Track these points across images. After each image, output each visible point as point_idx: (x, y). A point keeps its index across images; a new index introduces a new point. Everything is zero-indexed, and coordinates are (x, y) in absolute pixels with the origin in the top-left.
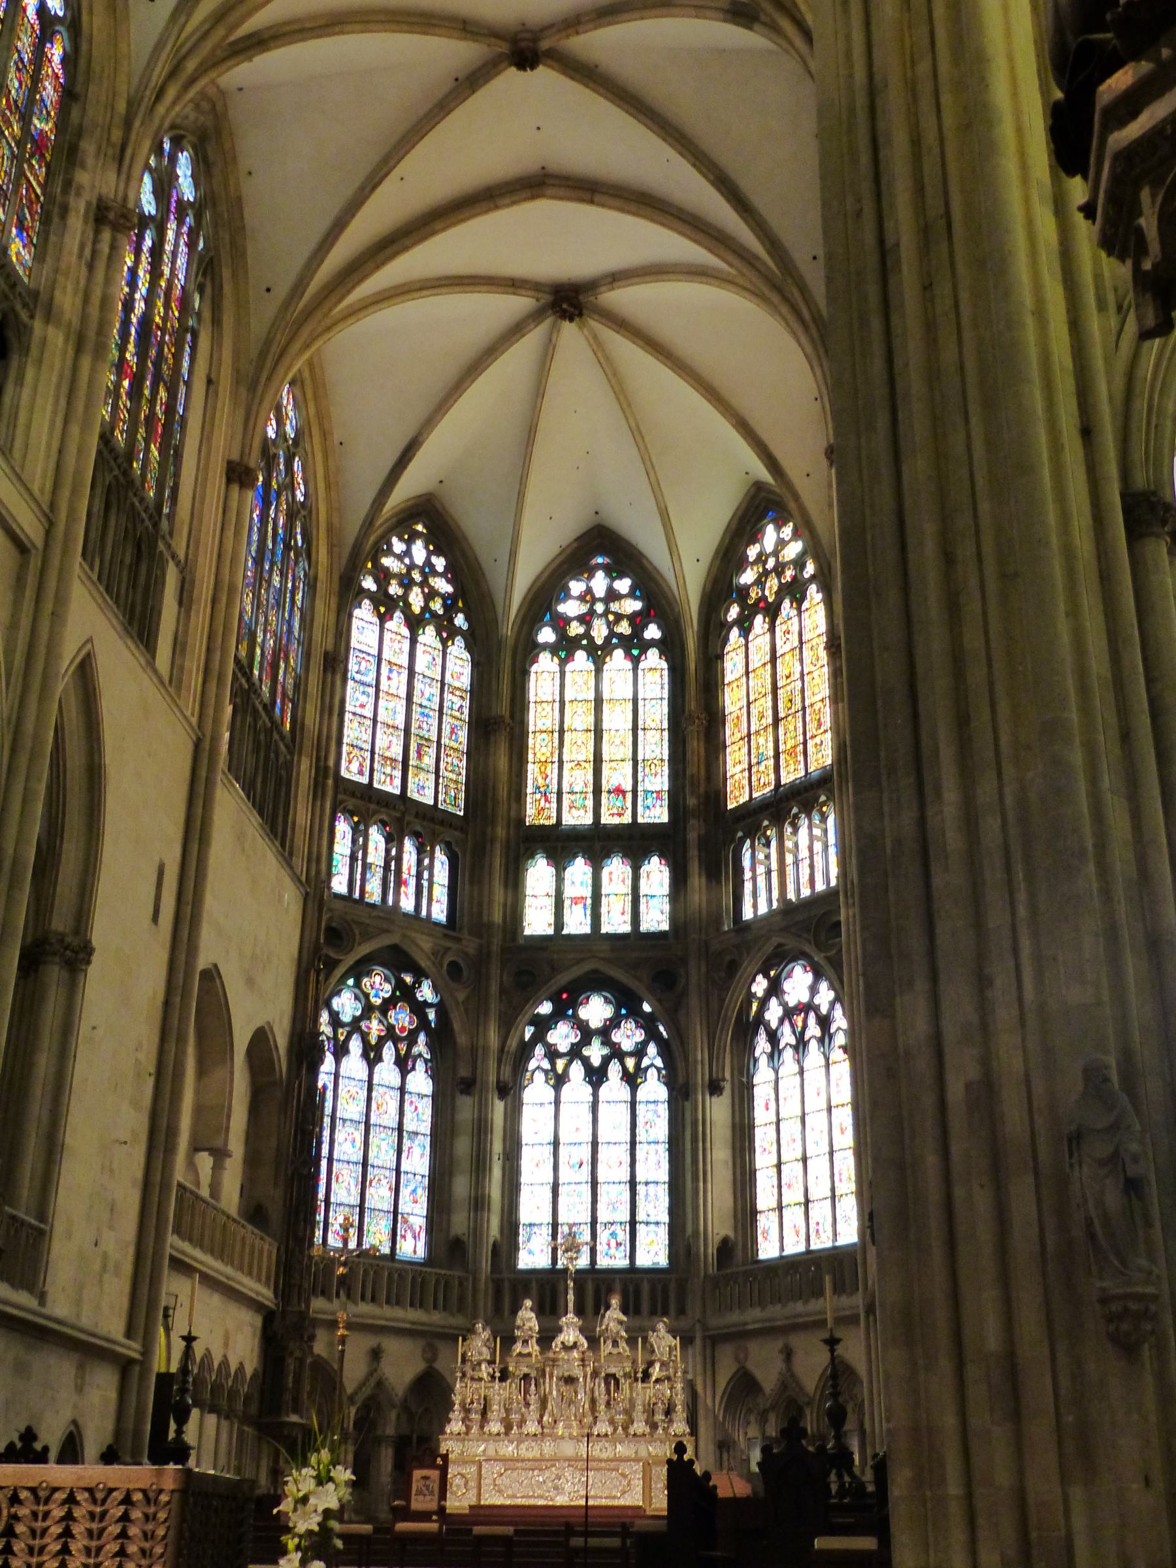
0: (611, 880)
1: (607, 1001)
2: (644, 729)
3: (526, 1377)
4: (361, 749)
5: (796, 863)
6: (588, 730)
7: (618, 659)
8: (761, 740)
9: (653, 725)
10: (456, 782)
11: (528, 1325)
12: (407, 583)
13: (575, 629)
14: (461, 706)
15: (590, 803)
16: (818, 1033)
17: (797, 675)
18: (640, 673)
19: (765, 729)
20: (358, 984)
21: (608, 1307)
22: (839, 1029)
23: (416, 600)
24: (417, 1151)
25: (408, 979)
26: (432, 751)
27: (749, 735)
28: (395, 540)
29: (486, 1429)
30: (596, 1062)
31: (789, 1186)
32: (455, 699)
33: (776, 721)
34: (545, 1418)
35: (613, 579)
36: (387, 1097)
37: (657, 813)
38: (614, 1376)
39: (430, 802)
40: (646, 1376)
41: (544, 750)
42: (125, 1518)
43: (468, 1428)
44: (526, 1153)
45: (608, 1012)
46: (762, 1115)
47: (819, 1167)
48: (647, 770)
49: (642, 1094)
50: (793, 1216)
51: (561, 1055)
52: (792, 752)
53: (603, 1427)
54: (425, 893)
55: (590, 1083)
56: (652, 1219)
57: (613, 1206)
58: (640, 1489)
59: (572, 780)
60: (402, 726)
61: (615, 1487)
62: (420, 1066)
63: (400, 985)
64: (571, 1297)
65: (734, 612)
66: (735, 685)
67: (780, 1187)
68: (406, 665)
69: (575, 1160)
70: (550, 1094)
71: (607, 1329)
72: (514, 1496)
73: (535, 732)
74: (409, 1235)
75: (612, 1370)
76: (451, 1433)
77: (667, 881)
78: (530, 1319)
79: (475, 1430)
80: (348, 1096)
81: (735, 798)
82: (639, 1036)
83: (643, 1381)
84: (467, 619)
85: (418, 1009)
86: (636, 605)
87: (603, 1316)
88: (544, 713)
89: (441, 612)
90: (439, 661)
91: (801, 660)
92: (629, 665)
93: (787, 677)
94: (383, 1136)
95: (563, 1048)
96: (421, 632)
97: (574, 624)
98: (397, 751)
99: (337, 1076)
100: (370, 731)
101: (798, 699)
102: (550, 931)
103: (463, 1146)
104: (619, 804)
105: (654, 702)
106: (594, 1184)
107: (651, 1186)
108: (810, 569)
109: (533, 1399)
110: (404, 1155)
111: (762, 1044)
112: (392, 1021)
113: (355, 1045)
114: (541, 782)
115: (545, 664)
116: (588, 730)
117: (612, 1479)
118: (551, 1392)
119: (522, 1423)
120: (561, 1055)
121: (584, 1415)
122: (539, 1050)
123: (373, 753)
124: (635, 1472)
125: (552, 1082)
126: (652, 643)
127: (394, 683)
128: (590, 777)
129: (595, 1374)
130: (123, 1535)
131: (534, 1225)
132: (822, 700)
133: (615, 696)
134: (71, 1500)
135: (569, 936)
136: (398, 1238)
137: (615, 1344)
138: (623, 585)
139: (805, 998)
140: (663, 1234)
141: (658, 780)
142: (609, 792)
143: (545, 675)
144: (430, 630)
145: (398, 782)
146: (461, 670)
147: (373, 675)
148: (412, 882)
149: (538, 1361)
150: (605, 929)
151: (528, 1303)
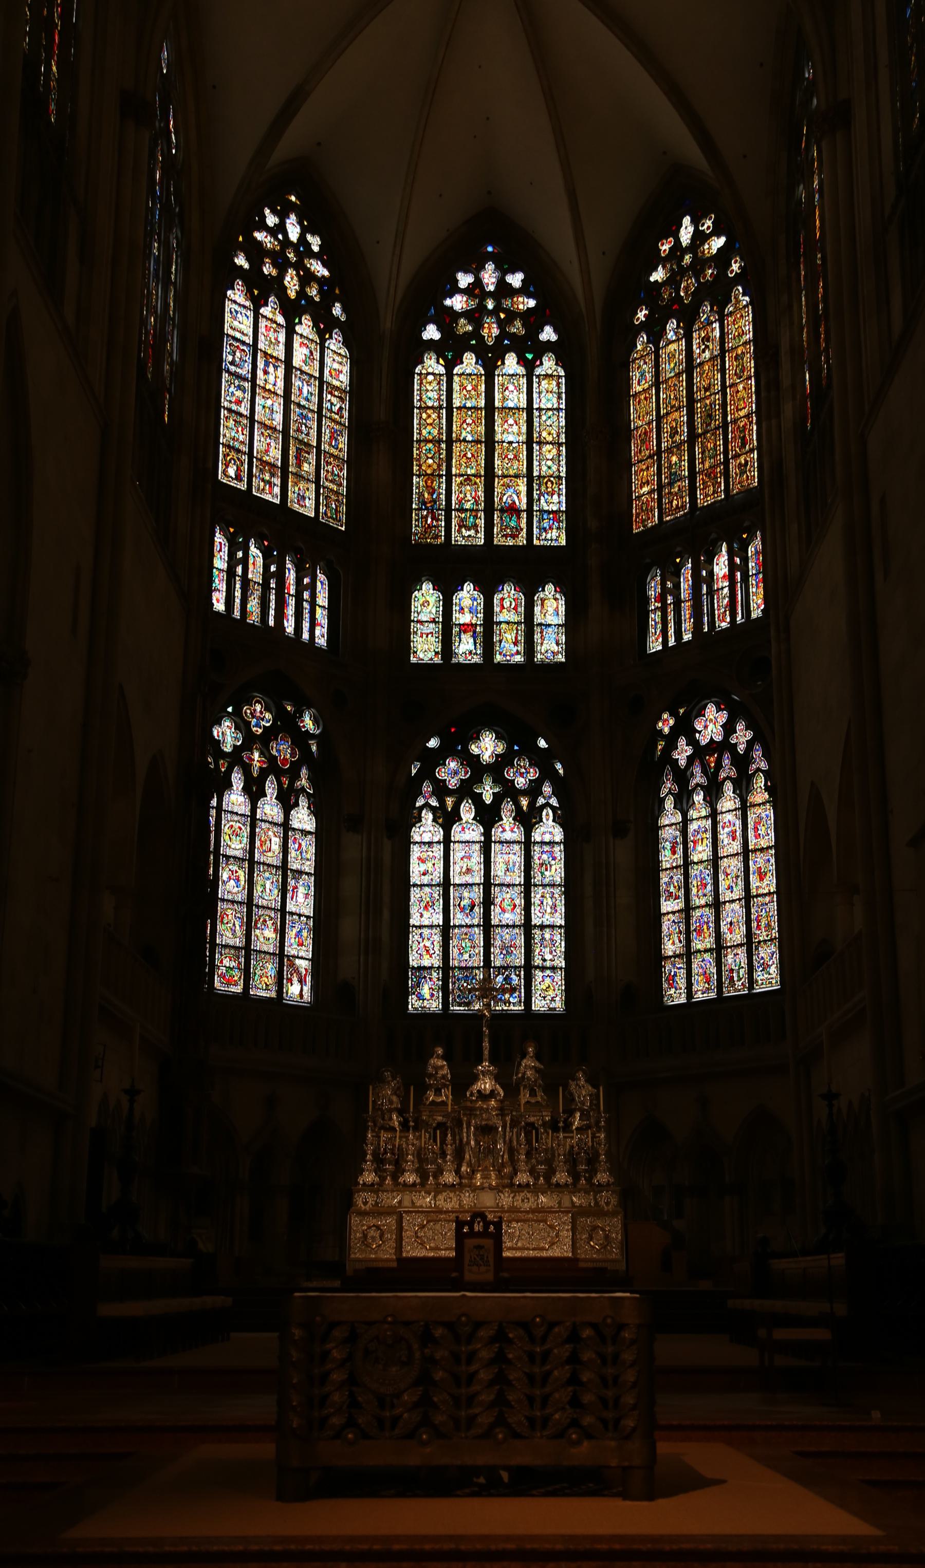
0: (503, 607)
1: (499, 737)
2: (540, 443)
3: (440, 1125)
4: (238, 451)
5: (711, 593)
6: (478, 442)
7: (511, 363)
8: (674, 459)
9: (550, 439)
10: (337, 493)
11: (441, 1073)
12: (282, 265)
13: (464, 326)
14: (341, 409)
15: (481, 522)
16: (733, 773)
17: (718, 387)
18: (535, 380)
19: (679, 446)
20: (237, 713)
21: (524, 1055)
22: (758, 770)
23: (291, 282)
24: (301, 891)
25: (289, 708)
26: (312, 458)
27: (659, 452)
28: (267, 211)
29: (401, 1180)
30: (488, 798)
31: (699, 932)
32: (334, 400)
33: (693, 437)
34: (463, 1169)
35: (504, 273)
36: (270, 833)
37: (556, 536)
38: (532, 1125)
39: (313, 515)
40: (567, 1127)
41: (430, 461)
42: (574, 1359)
43: (383, 1179)
44: (415, 894)
45: (500, 749)
46: (667, 858)
47: (733, 912)
48: (543, 489)
49: (536, 836)
50: (704, 964)
51: (450, 793)
52: (710, 474)
53: (523, 1178)
54: (306, 616)
55: (481, 822)
56: (548, 964)
57: (507, 950)
58: (568, 1241)
59: (462, 496)
60: (280, 428)
61: (544, 1238)
62: (303, 802)
63: (279, 713)
64: (486, 1044)
65: (642, 315)
66: (642, 397)
67: (688, 932)
68: (282, 357)
69: (465, 902)
70: (439, 835)
71: (523, 1077)
72: (437, 1249)
73: (419, 441)
74: (295, 980)
75: (532, 1119)
76: (364, 1184)
77: (562, 609)
78: (443, 1066)
79: (388, 1181)
80: (230, 832)
81: (643, 521)
82: (533, 774)
83: (564, 1132)
84: (344, 309)
85: (300, 739)
86: (532, 303)
87: (520, 1064)
88: (429, 421)
89: (317, 299)
90: (317, 355)
91: (723, 371)
92: (521, 370)
93: (706, 390)
94: (267, 875)
95: (453, 783)
96: (297, 321)
97: (462, 321)
98: (275, 454)
99: (219, 808)
100: (246, 432)
101: (718, 416)
102: (438, 660)
103: (351, 886)
104: (513, 524)
105: (550, 413)
106: (487, 927)
107: (548, 930)
108: (735, 267)
109: (449, 1149)
110: (289, 895)
111: (668, 786)
112: (274, 752)
113: (237, 780)
114: (426, 495)
115: (432, 365)
116: (478, 442)
117: (540, 1230)
118: (468, 1143)
119: (439, 1172)
120: (450, 793)
121: (503, 1165)
122: (427, 787)
123: (250, 455)
124: (564, 1223)
125: (440, 821)
126: (548, 346)
127: (271, 379)
128: (481, 493)
129: (514, 1123)
130: (574, 1380)
131: (425, 968)
132: (747, 416)
133: (511, 405)
134: (500, 1337)
135: (459, 664)
136: (285, 981)
137: (533, 1093)
138: (516, 280)
139: (718, 738)
140: (559, 977)
141: (556, 501)
142: (502, 511)
143: (430, 378)
144: (307, 321)
145: (277, 490)
146: (340, 368)
147: (248, 367)
148: (292, 602)
149: (453, 1110)
150: (498, 658)
151: (440, 1051)
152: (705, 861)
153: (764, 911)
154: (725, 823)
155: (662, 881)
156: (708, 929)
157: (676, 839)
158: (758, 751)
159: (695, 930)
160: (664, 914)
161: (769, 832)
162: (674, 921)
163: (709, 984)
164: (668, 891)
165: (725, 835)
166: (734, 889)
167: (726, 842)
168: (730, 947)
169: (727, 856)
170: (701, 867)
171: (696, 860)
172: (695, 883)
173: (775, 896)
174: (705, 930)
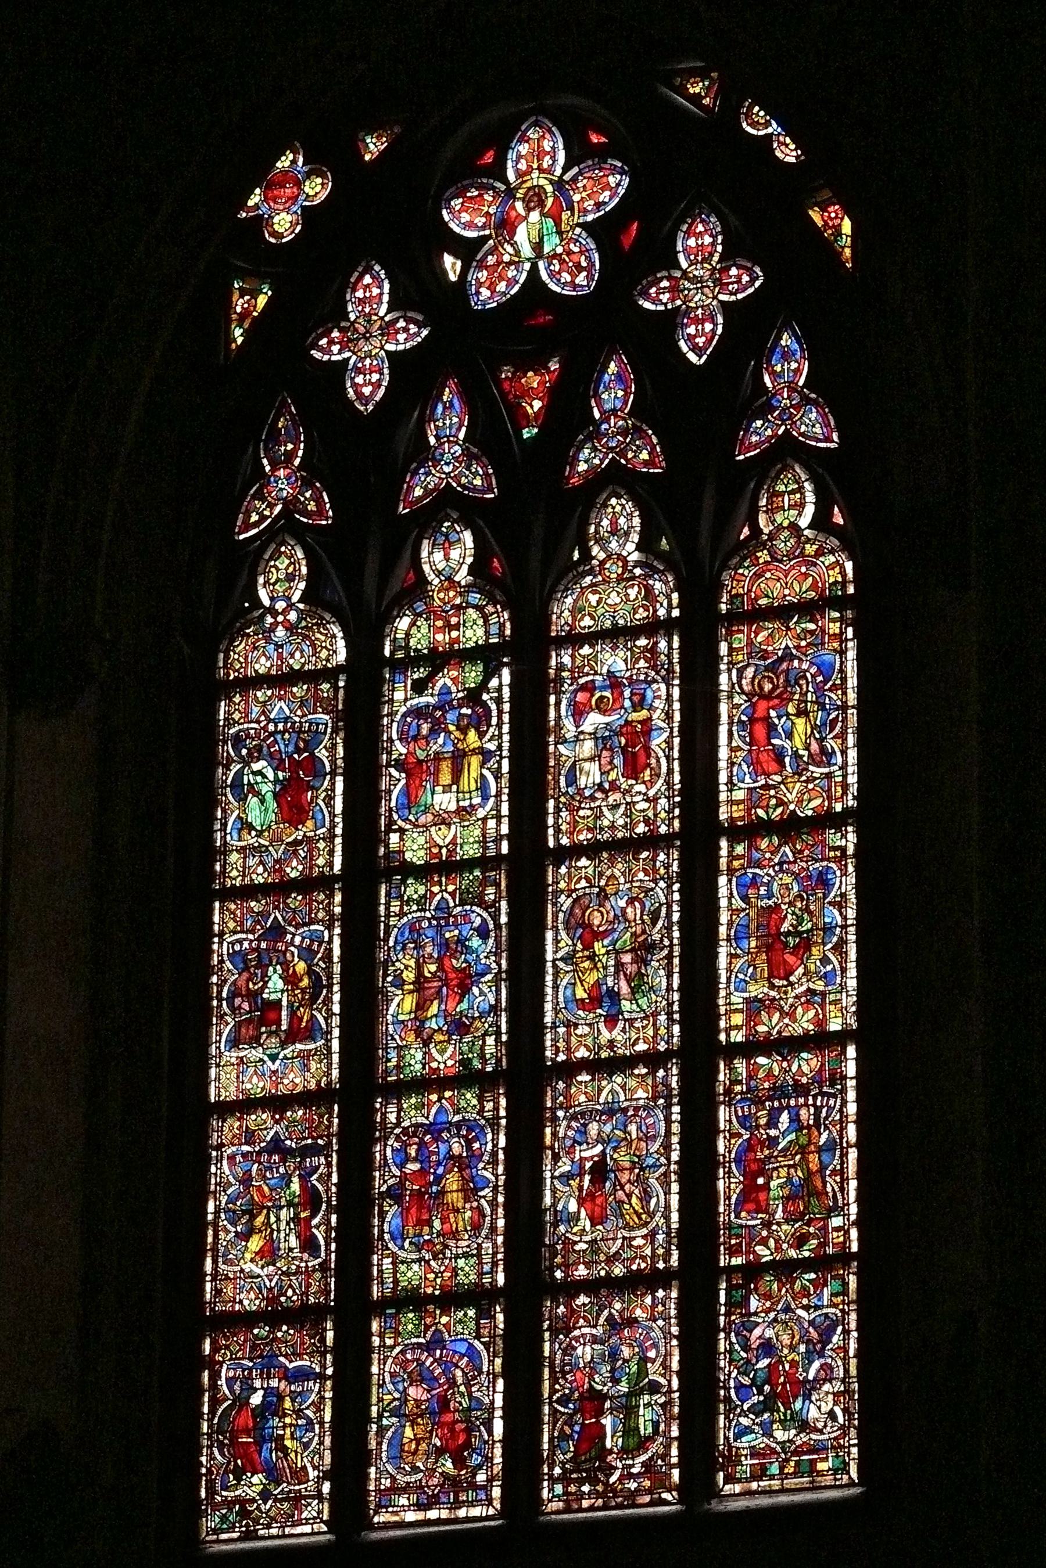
152: (469, 864)
153: (785, 1117)
154: (589, 688)
155: (220, 949)
156: (470, 1191)
157: (310, 746)
158: (787, 356)
159: (395, 1194)
160: (226, 1109)
161: (831, 744)
162: (276, 1146)
163: (459, 1462)
164: (253, 996)
165: (588, 747)
166: (626, 1005)
167: (591, 775)
168: (589, 1286)
169: (592, 850)
170: (443, 891)
171: (416, 855)
172: (406, 965)
173: (851, 1051)
174: (455, 1198)
